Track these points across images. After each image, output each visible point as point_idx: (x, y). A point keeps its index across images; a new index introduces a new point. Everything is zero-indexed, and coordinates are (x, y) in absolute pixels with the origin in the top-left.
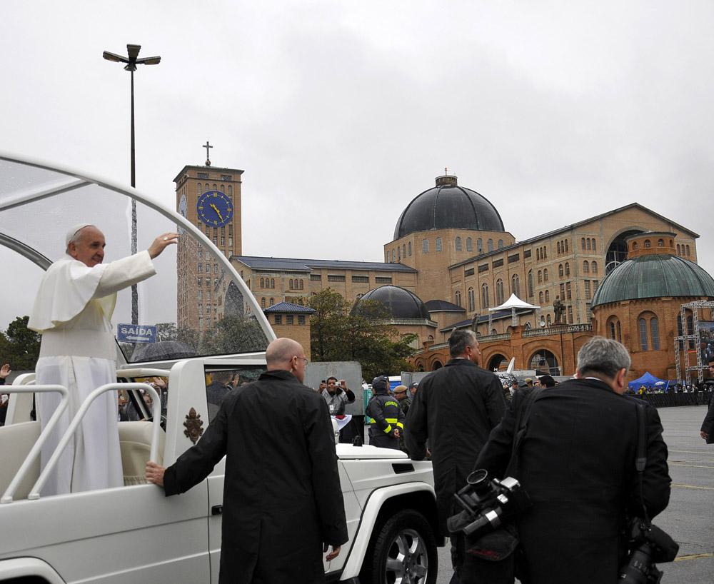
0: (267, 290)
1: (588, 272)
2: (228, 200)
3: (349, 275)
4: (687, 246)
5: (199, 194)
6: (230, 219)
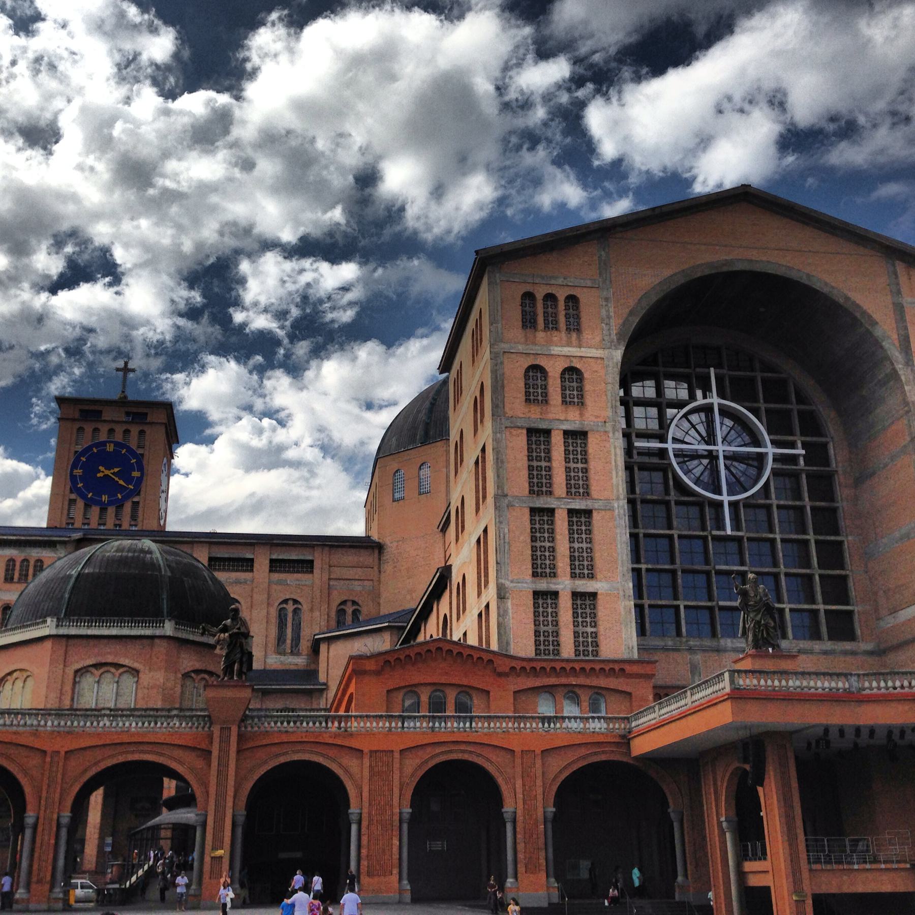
1: (546, 401)
5: (79, 448)
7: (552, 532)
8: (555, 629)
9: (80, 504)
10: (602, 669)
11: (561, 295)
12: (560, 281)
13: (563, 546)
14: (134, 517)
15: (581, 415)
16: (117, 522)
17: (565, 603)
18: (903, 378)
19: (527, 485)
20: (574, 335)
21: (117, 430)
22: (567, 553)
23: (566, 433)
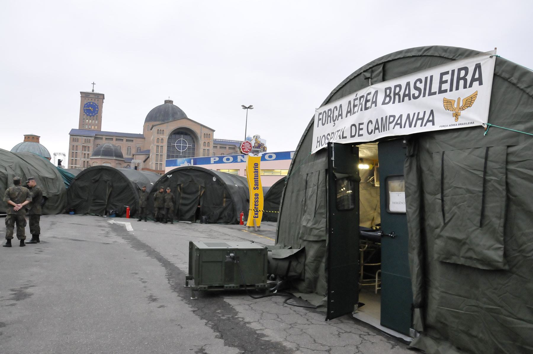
0: (76, 143)
2: (97, 105)
3: (114, 138)
4: (209, 134)
5: (85, 103)
6: (97, 113)
9: (86, 115)
17: (159, 164)
23: (161, 146)
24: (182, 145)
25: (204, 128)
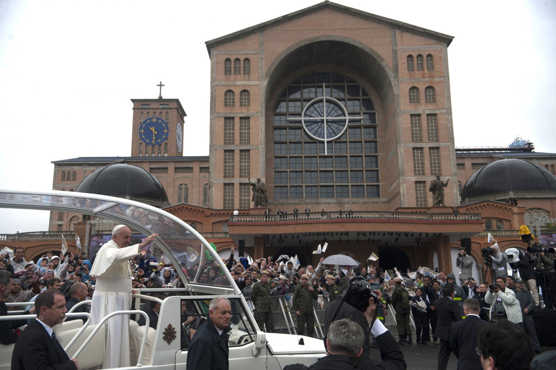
0: (67, 182)
4: (430, 56)
7: (233, 159)
8: (232, 198)
9: (144, 144)
10: (228, 214)
11: (242, 59)
12: (242, 52)
13: (237, 165)
14: (166, 150)
15: (248, 110)
16: (159, 152)
17: (237, 187)
18: (393, 84)
19: (223, 141)
20: (247, 76)
21: (157, 112)
22: (239, 167)
23: (241, 118)
24: (325, 118)
25: (407, 36)
